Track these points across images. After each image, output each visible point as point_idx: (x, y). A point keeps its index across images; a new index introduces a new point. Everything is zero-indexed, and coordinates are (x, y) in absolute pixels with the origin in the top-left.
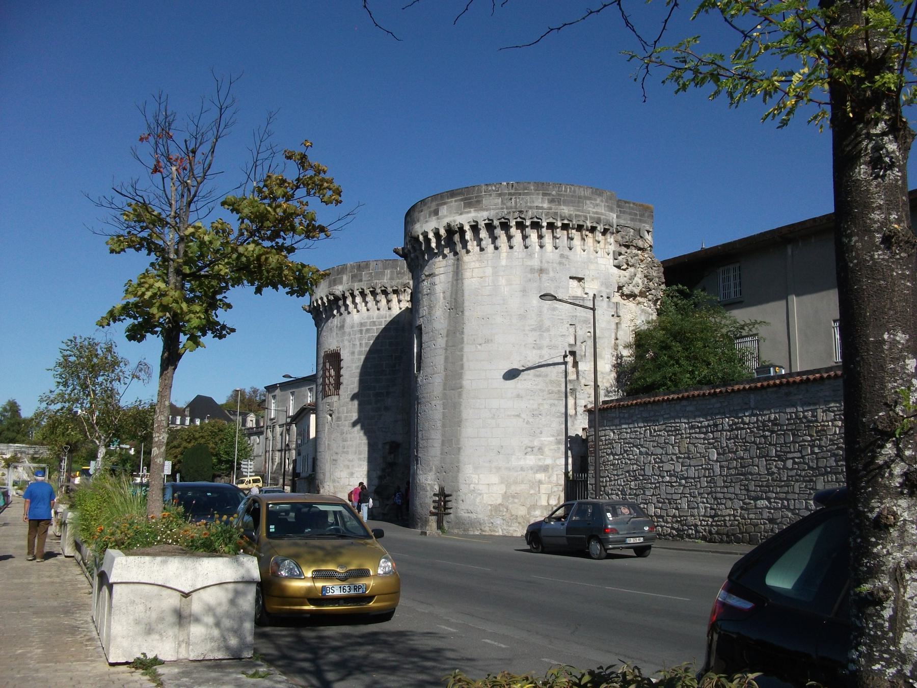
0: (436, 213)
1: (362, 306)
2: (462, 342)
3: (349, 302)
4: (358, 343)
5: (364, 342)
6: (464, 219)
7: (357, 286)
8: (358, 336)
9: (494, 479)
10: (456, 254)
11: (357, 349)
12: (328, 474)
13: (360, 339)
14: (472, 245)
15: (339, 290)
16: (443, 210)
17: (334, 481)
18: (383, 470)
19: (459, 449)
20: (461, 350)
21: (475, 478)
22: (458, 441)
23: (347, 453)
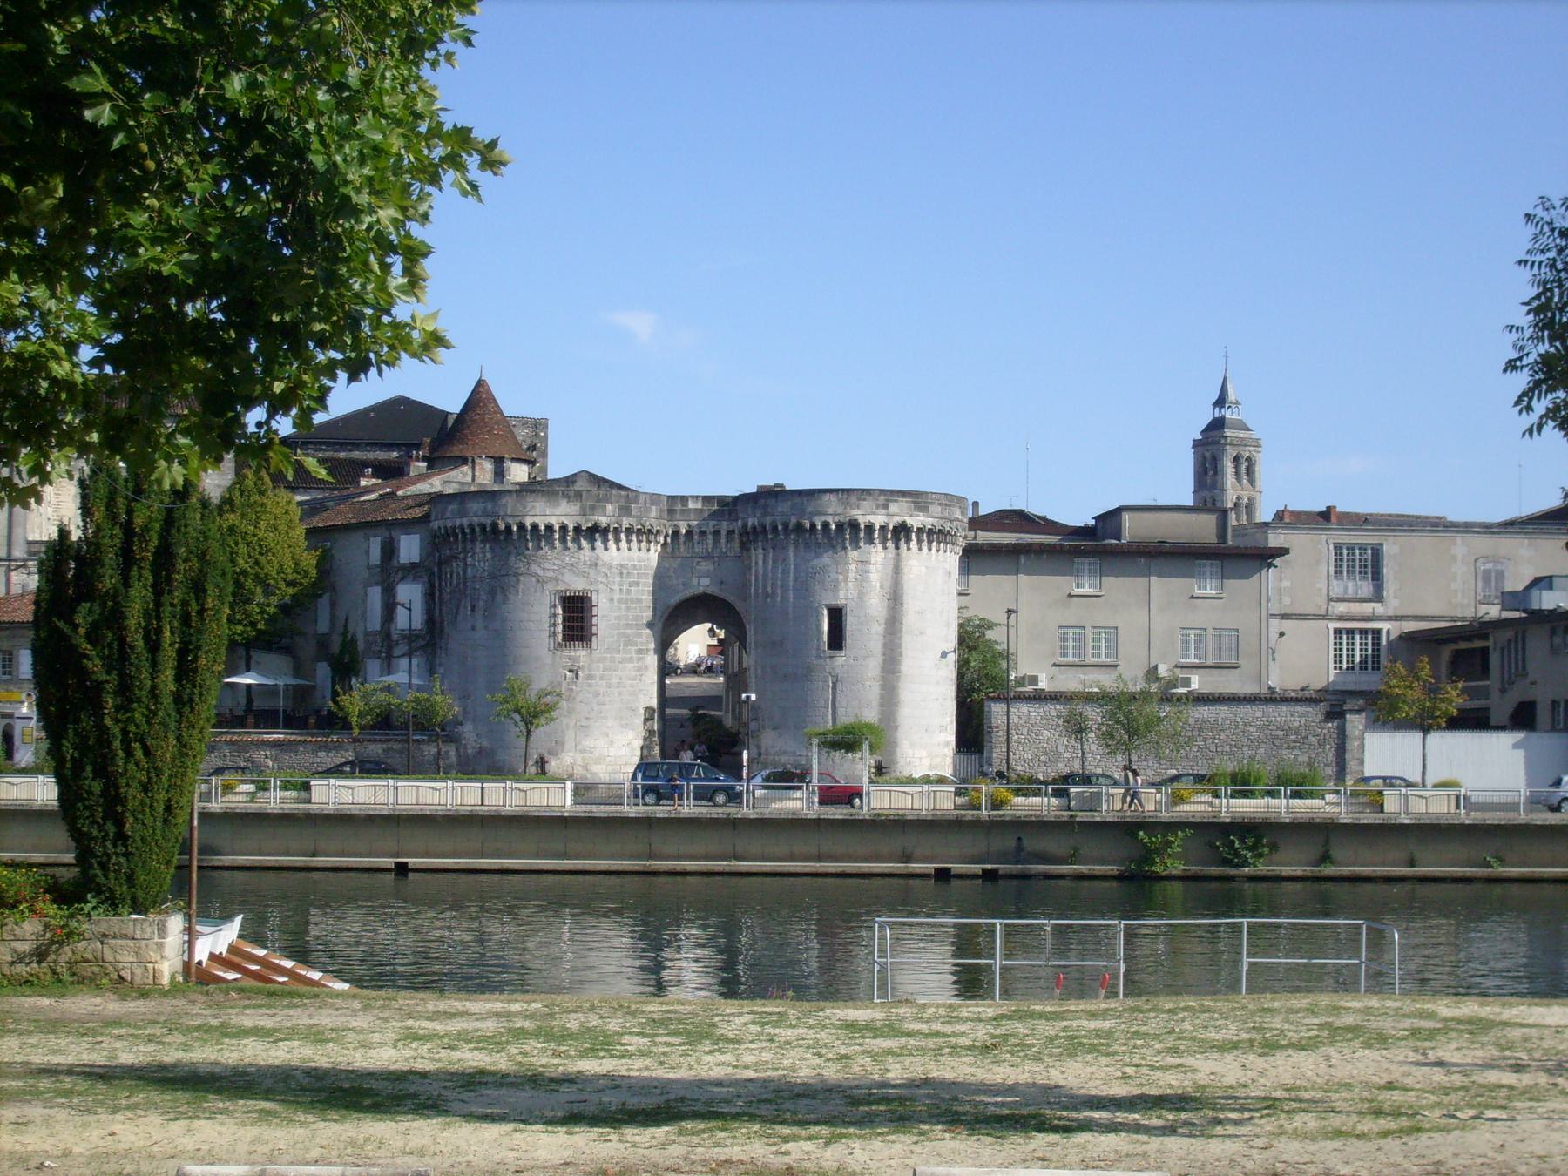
0: (886, 507)
1: (623, 544)
2: (901, 631)
3: (610, 536)
4: (617, 588)
5: (624, 588)
6: (915, 521)
7: (625, 522)
8: (618, 579)
9: (924, 753)
10: (897, 547)
11: (617, 596)
12: (569, 744)
13: (621, 584)
14: (914, 544)
15: (603, 521)
16: (893, 507)
17: (583, 751)
18: (645, 739)
19: (897, 727)
20: (900, 638)
21: (910, 752)
22: (895, 720)
23: (606, 718)
